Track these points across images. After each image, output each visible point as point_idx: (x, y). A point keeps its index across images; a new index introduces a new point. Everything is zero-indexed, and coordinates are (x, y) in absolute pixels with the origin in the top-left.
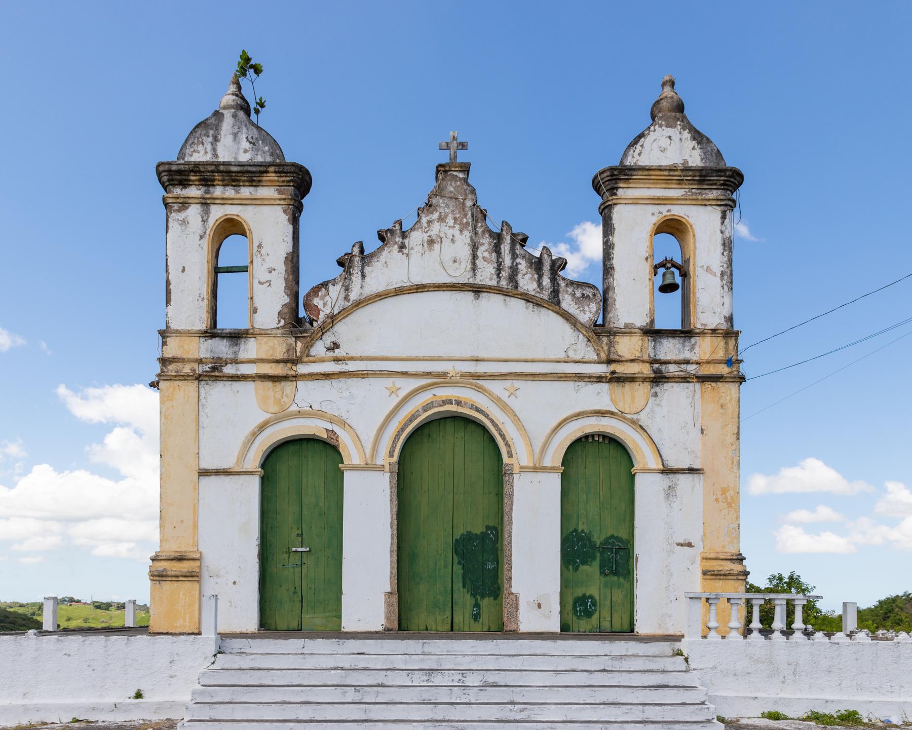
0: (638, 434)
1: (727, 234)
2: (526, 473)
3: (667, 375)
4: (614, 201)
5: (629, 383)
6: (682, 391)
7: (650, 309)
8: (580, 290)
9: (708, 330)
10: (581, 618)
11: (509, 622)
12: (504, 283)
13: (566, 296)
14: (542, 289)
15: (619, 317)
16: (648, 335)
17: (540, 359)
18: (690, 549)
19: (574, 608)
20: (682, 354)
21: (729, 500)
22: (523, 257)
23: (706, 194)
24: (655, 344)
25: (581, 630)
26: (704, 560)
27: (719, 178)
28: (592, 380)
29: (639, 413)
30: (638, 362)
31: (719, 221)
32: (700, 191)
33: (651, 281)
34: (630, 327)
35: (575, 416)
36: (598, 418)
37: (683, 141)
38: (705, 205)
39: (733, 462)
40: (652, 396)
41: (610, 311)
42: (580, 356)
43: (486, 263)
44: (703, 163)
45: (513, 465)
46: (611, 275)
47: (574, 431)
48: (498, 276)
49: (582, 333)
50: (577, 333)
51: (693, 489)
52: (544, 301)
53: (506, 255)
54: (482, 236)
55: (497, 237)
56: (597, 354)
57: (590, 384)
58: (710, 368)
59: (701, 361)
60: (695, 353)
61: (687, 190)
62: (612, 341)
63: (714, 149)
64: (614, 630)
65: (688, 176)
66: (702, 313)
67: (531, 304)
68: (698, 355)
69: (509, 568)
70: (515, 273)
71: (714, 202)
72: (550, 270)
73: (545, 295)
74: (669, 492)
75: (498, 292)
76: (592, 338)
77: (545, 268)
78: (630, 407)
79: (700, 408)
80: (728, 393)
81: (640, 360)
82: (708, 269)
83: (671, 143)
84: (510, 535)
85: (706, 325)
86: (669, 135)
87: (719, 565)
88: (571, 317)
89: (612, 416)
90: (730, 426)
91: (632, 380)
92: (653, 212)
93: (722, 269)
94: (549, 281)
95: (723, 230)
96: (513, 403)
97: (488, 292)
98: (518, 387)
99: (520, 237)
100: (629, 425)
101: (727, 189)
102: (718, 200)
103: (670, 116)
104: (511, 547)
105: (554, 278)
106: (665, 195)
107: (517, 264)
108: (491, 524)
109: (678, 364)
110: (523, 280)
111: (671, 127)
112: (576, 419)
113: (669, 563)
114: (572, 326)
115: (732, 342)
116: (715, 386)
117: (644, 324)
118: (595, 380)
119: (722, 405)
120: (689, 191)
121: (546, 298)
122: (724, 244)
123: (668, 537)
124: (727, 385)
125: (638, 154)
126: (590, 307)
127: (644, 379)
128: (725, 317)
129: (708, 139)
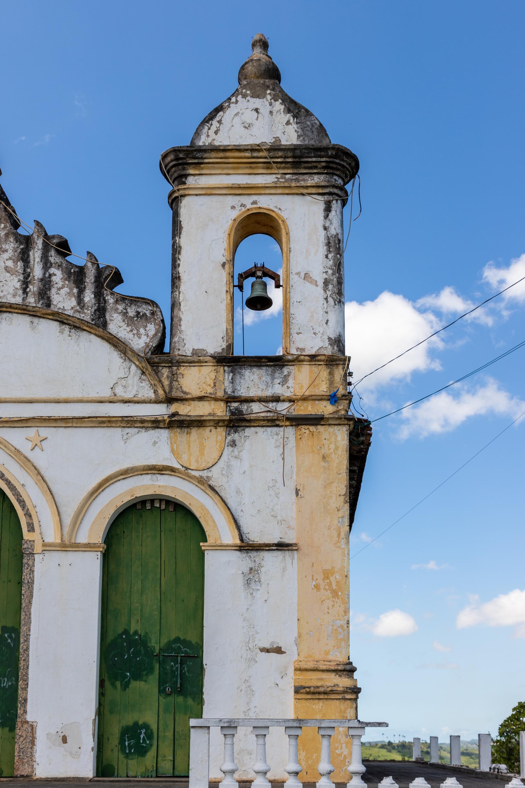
0: (209, 497)
1: (333, 231)
2: (51, 552)
3: (247, 417)
4: (181, 192)
5: (196, 428)
6: (270, 437)
7: (227, 330)
8: (133, 308)
9: (305, 356)
10: (131, 757)
11: (21, 763)
12: (31, 300)
13: (115, 315)
14: (82, 307)
15: (185, 342)
16: (224, 364)
17: (76, 399)
18: (279, 656)
19: (122, 742)
20: (270, 389)
21: (334, 587)
22: (59, 266)
23: (304, 180)
24: (233, 376)
25: (131, 773)
26: (298, 672)
27: (319, 159)
28: (146, 425)
29: (210, 469)
30: (208, 401)
31: (321, 214)
32: (297, 177)
33: (228, 293)
34: (200, 355)
35: (122, 475)
36: (154, 477)
37: (275, 113)
38: (303, 194)
39: (339, 535)
40: (228, 446)
41: (175, 335)
42: (132, 393)
43: (8, 275)
44: (301, 141)
45: (34, 541)
46: (177, 287)
47: (120, 495)
48: (25, 291)
49: (134, 363)
50: (128, 363)
51: (284, 571)
52: (83, 322)
53: (36, 265)
54: (6, 240)
55: (24, 242)
56: (155, 390)
57: (143, 430)
58: (308, 406)
59: (295, 397)
60: (288, 387)
61: (279, 176)
62: (174, 373)
63: (315, 123)
64: (177, 773)
65: (278, 158)
66: (298, 334)
67: (67, 326)
68: (292, 390)
69: (24, 686)
70: (47, 286)
71: (314, 191)
72: (95, 282)
73: (87, 315)
74: (251, 576)
75: (22, 312)
76: (147, 369)
77: (87, 280)
78: (197, 461)
79: (295, 461)
80: (333, 439)
81: (210, 397)
82: (307, 277)
83: (258, 117)
84: (27, 639)
85: (303, 350)
86: (255, 106)
87: (317, 679)
88: (118, 343)
89: (172, 473)
90: (335, 484)
91: (199, 424)
92: (233, 204)
93: (325, 276)
94: (93, 296)
95: (327, 225)
96: (37, 457)
97: (10, 312)
98: (45, 436)
99: (55, 241)
100: (196, 486)
101: (333, 174)
102: (318, 187)
103: (257, 84)
104: (28, 656)
105: (100, 292)
106: (249, 182)
107: (50, 275)
108: (8, 625)
109: (264, 401)
110: (58, 295)
111: (258, 97)
112: (124, 479)
113: (250, 677)
114: (122, 355)
115: (339, 372)
116: (315, 430)
117: (219, 350)
118: (150, 425)
119: (324, 456)
120: (282, 178)
121: (88, 318)
122: (328, 244)
123: (247, 640)
124: (331, 429)
125: (215, 133)
126: (147, 329)
127: (217, 423)
128: (330, 339)
129: (307, 111)
